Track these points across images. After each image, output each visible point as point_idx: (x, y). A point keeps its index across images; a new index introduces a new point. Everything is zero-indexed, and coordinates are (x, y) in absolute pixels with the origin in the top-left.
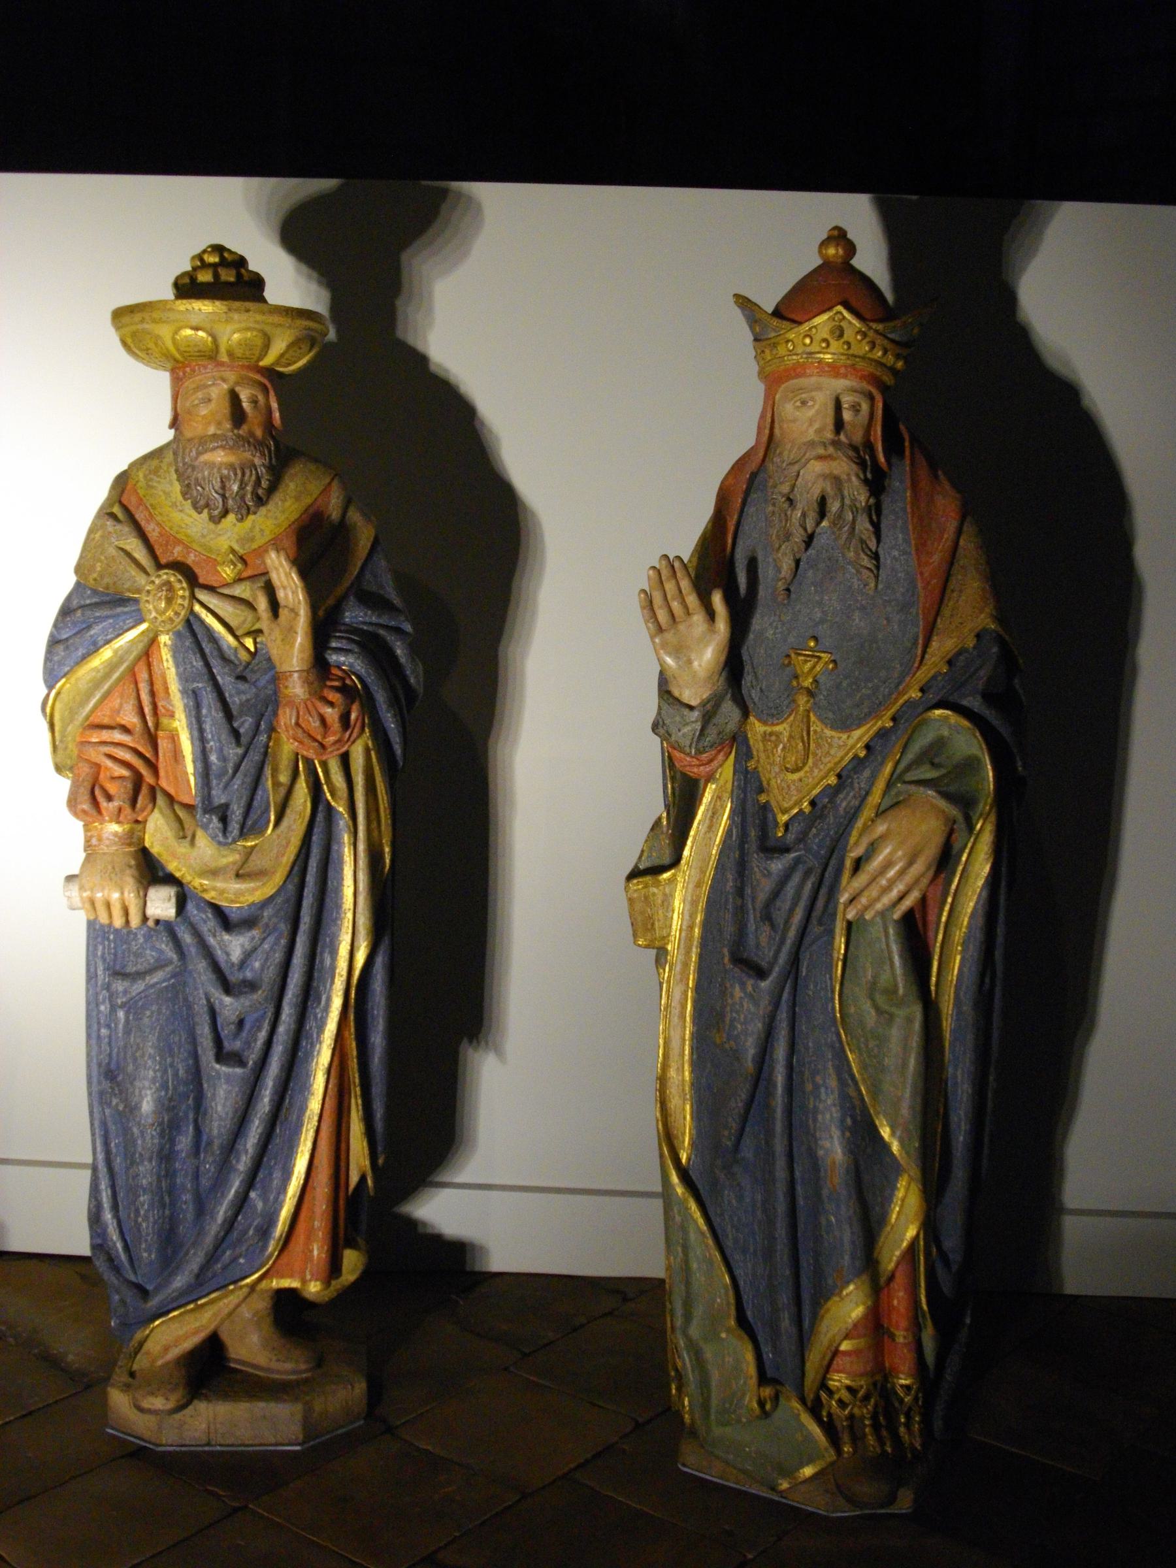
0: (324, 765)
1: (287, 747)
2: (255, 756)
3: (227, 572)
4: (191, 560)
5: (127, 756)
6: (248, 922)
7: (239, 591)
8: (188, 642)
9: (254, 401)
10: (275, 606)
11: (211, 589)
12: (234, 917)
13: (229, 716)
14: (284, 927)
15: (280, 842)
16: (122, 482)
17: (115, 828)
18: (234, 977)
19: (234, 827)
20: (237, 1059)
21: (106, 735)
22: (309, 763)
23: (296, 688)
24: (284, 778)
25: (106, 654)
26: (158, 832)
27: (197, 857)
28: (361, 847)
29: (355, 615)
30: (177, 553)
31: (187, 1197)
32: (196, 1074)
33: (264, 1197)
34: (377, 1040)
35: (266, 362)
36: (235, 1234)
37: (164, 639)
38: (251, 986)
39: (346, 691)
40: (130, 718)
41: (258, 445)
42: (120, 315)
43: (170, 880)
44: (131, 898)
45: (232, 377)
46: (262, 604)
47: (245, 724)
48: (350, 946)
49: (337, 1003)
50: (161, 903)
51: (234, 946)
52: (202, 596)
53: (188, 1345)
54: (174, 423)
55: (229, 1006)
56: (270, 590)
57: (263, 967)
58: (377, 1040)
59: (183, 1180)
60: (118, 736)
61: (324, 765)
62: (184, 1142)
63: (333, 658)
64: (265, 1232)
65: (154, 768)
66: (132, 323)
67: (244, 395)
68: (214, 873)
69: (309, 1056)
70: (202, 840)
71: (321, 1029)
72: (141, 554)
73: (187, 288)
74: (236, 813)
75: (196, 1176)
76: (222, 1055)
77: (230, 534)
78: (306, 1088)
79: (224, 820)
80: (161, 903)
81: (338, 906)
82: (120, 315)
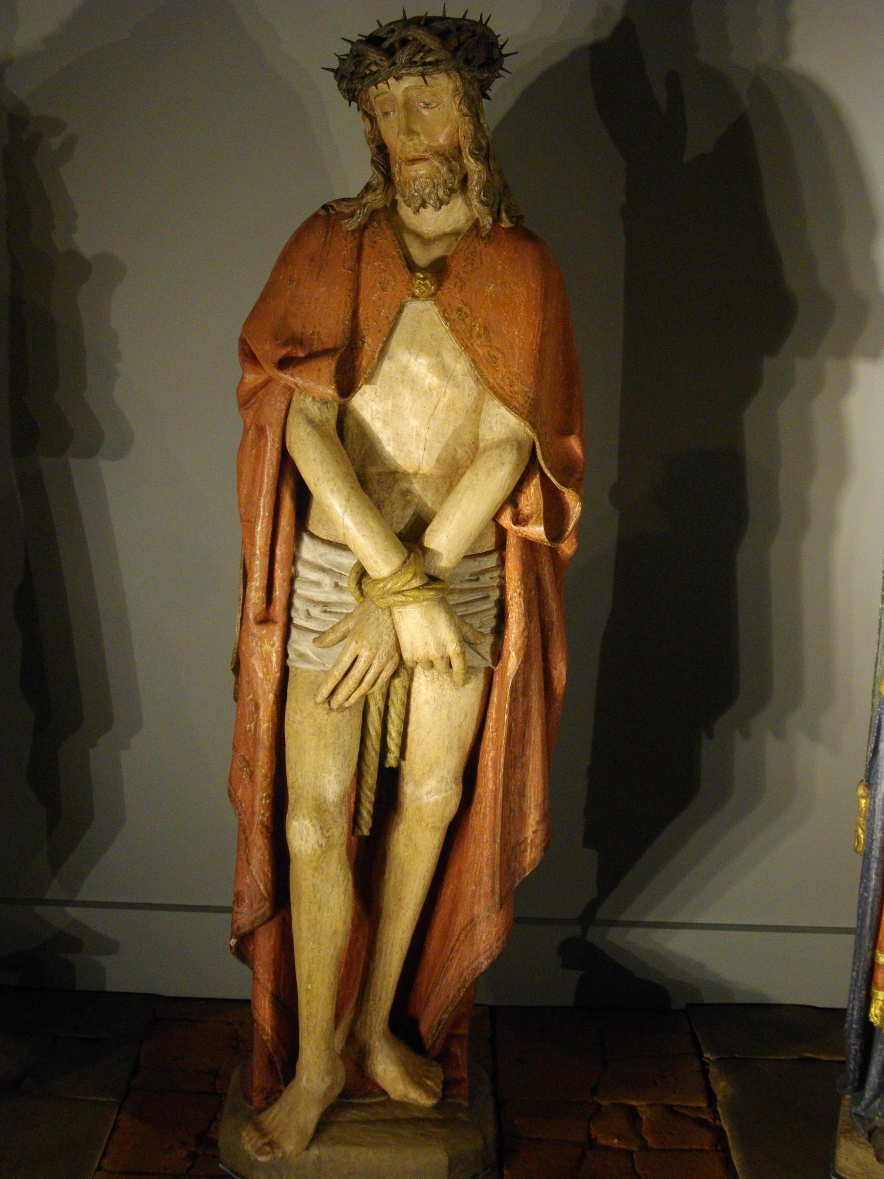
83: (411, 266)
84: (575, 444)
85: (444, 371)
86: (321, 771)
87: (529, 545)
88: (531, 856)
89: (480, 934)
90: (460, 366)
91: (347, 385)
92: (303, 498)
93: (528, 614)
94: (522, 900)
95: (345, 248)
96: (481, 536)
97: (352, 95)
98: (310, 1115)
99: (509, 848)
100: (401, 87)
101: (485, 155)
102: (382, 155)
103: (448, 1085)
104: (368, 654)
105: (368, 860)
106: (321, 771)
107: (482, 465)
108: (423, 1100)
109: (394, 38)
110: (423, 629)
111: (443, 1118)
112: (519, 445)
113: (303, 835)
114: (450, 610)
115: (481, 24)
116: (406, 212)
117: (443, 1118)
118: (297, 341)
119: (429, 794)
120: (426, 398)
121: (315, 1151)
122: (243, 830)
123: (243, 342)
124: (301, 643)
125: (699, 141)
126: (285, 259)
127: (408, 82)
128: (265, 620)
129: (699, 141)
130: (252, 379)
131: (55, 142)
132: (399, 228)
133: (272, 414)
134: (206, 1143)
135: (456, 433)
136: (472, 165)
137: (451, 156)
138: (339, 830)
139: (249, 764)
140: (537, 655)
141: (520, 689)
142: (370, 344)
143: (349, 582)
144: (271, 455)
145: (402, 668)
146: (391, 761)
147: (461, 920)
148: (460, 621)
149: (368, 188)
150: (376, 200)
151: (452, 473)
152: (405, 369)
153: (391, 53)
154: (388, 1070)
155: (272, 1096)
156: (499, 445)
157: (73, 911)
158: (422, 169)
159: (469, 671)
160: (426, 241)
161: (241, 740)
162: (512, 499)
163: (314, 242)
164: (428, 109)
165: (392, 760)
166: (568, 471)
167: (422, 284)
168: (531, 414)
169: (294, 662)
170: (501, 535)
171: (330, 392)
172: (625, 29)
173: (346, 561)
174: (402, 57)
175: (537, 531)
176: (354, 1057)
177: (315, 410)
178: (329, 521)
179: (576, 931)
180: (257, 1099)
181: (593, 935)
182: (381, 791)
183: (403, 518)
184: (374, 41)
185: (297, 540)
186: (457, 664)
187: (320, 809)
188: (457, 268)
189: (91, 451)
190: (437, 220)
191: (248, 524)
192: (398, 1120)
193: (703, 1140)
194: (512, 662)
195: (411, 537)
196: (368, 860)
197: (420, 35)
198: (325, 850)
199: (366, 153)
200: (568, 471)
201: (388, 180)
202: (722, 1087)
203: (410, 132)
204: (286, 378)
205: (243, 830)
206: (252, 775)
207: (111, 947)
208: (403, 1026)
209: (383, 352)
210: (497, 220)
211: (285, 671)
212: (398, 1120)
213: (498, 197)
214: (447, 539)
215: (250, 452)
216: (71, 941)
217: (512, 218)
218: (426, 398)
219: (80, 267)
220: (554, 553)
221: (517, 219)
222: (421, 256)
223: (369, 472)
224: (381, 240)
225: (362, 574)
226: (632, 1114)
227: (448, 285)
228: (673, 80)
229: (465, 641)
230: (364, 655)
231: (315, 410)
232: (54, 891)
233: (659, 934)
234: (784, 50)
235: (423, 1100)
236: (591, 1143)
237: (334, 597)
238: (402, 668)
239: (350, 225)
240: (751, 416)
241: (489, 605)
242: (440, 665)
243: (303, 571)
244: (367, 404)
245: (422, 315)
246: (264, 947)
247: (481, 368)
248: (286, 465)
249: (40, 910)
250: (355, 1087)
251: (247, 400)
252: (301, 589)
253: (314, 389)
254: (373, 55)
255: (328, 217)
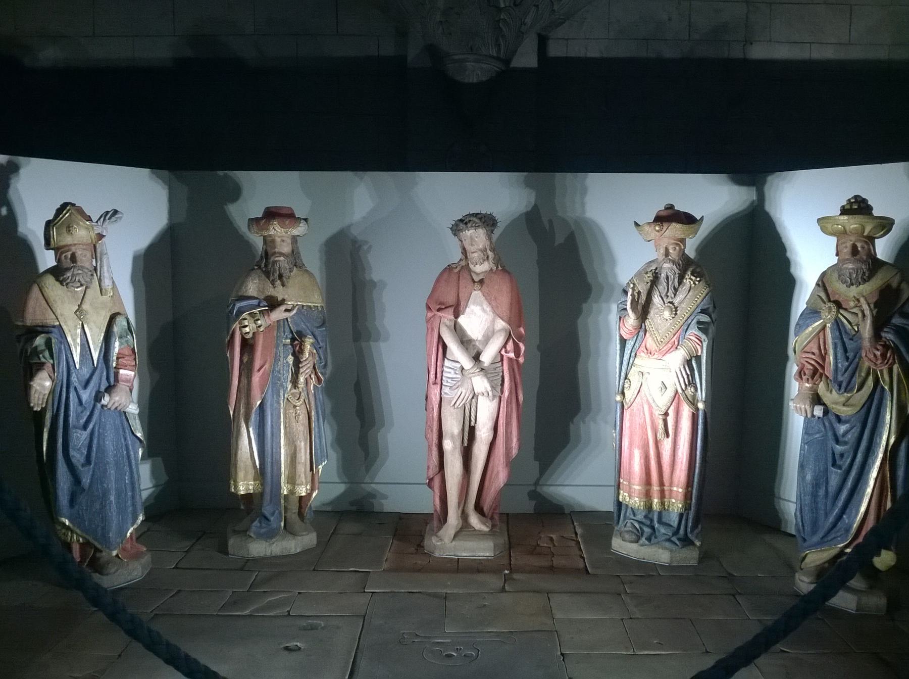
0: (881, 371)
1: (867, 364)
2: (853, 366)
3: (852, 304)
4: (840, 300)
5: (813, 362)
6: (846, 422)
7: (854, 310)
8: (835, 327)
9: (863, 247)
10: (864, 316)
11: (846, 309)
12: (843, 419)
13: (845, 350)
14: (859, 425)
15: (861, 397)
16: (824, 274)
17: (807, 385)
18: (841, 439)
19: (843, 390)
20: (840, 468)
21: (807, 355)
22: (875, 372)
23: (866, 344)
24: (863, 374)
25: (810, 329)
26: (822, 388)
27: (832, 397)
28: (895, 402)
29: (897, 320)
30: (836, 298)
31: (822, 512)
32: (826, 470)
33: (849, 518)
34: (901, 473)
35: (865, 234)
36: (835, 530)
37: (828, 325)
38: (845, 443)
39: (886, 347)
40: (816, 351)
41: (862, 261)
42: (819, 220)
43: (824, 404)
44: (808, 407)
45: (853, 238)
46: (860, 315)
47: (851, 355)
48: (886, 436)
49: (881, 455)
50: (818, 411)
51: (842, 428)
52: (842, 311)
53: (818, 563)
54: (837, 255)
55: (839, 448)
56: (863, 312)
57: (851, 437)
58: (901, 473)
59: (821, 506)
60: (813, 357)
61: (881, 371)
62: (822, 492)
63: (883, 334)
64: (847, 530)
65: (823, 367)
66: (823, 223)
67: (859, 245)
68: (836, 403)
69: (869, 472)
70: (834, 392)
71: (874, 463)
72: (824, 297)
73: (844, 211)
74: (844, 385)
75: (826, 506)
76: (834, 464)
77: (854, 291)
78: (867, 483)
79: (840, 386)
80: (818, 411)
81: (884, 422)
82: (819, 220)
83: (474, 282)
84: (522, 330)
85: (484, 310)
86: (453, 426)
87: (510, 359)
88: (515, 452)
89: (500, 475)
90: (488, 309)
91: (457, 315)
92: (445, 347)
93: (510, 379)
94: (512, 465)
95: (455, 277)
96: (496, 357)
97: (455, 235)
98: (452, 532)
99: (508, 449)
100: (469, 233)
101: (493, 250)
102: (464, 251)
103: (493, 526)
104: (464, 391)
105: (467, 454)
106: (453, 426)
107: (495, 337)
108: (485, 529)
109: (467, 220)
110: (481, 384)
111: (492, 533)
112: (506, 330)
113: (448, 445)
114: (488, 378)
115: (491, 214)
116: (471, 266)
117: (492, 533)
118: (441, 303)
119: (484, 434)
120: (479, 318)
121: (454, 543)
122: (430, 447)
123: (427, 305)
124: (446, 390)
125: (560, 239)
126: (438, 281)
127: (471, 231)
128: (435, 383)
129: (560, 239)
130: (430, 314)
131: (365, 247)
132: (470, 271)
133: (436, 325)
134: (420, 546)
135: (488, 328)
136: (490, 253)
137: (484, 251)
138: (458, 443)
139: (431, 427)
140: (514, 392)
141: (509, 402)
142: (462, 303)
143: (459, 372)
144: (436, 336)
145: (475, 396)
146: (472, 424)
147: (495, 473)
148: (491, 382)
149: (461, 260)
150: (463, 263)
151: (487, 339)
152: (472, 311)
153: (466, 223)
154: (475, 521)
155: (440, 528)
156: (500, 331)
157: (373, 485)
158: (475, 255)
159: (494, 396)
160: (477, 274)
161: (428, 420)
162: (505, 346)
163: (446, 276)
164: (477, 238)
165: (472, 424)
166: (520, 338)
167: (477, 286)
168: (509, 322)
169: (444, 396)
170: (502, 356)
171: (452, 317)
172: (535, 207)
173: (458, 365)
174: (469, 225)
175: (512, 355)
176: (464, 516)
177: (448, 323)
178: (453, 354)
179: (533, 488)
180: (435, 530)
181: (539, 489)
182: (471, 433)
183: (474, 353)
184: (461, 221)
185: (444, 360)
186: (490, 394)
187: (452, 437)
188: (486, 281)
189: (377, 340)
190: (481, 268)
191: (429, 356)
192: (479, 535)
193: (573, 544)
194: (506, 393)
195: (476, 358)
196: (467, 454)
197: (474, 219)
198: (454, 448)
199: (460, 250)
200: (520, 338)
201: (466, 257)
202: (579, 531)
203: (472, 245)
204: (439, 314)
205: (430, 447)
206: (432, 431)
207: (385, 497)
208: (478, 508)
209: (466, 306)
210: (497, 267)
211: (441, 398)
212: (479, 535)
213: (497, 261)
214: (487, 357)
215: (429, 335)
216: (372, 495)
217: (502, 267)
218: (479, 318)
219: (373, 284)
220: (517, 361)
221: (503, 267)
222: (476, 279)
223: (465, 341)
224: (465, 274)
225: (462, 369)
226: (551, 539)
227: (484, 286)
228: (550, 221)
229: (492, 387)
230: (464, 391)
231: (448, 323)
232: (367, 480)
233: (560, 488)
234: (584, 211)
235: (485, 529)
236: (538, 545)
237: (455, 376)
238: (475, 396)
239: (456, 271)
240: (580, 321)
241: (499, 377)
242: (486, 394)
243: (445, 369)
244: (462, 320)
245: (477, 294)
246: (437, 483)
247: (494, 310)
248: (440, 337)
249: (363, 485)
250: (465, 526)
251: (428, 321)
252: (444, 374)
253: (447, 317)
254: (462, 226)
255: (449, 269)
